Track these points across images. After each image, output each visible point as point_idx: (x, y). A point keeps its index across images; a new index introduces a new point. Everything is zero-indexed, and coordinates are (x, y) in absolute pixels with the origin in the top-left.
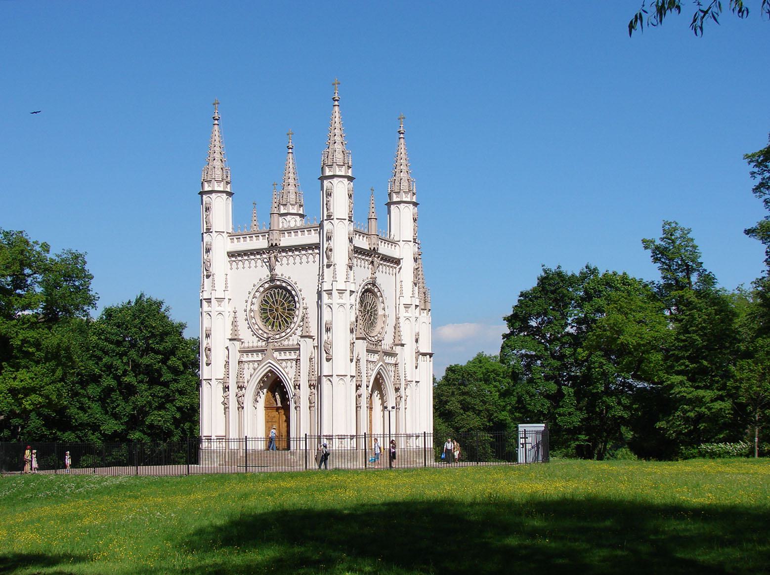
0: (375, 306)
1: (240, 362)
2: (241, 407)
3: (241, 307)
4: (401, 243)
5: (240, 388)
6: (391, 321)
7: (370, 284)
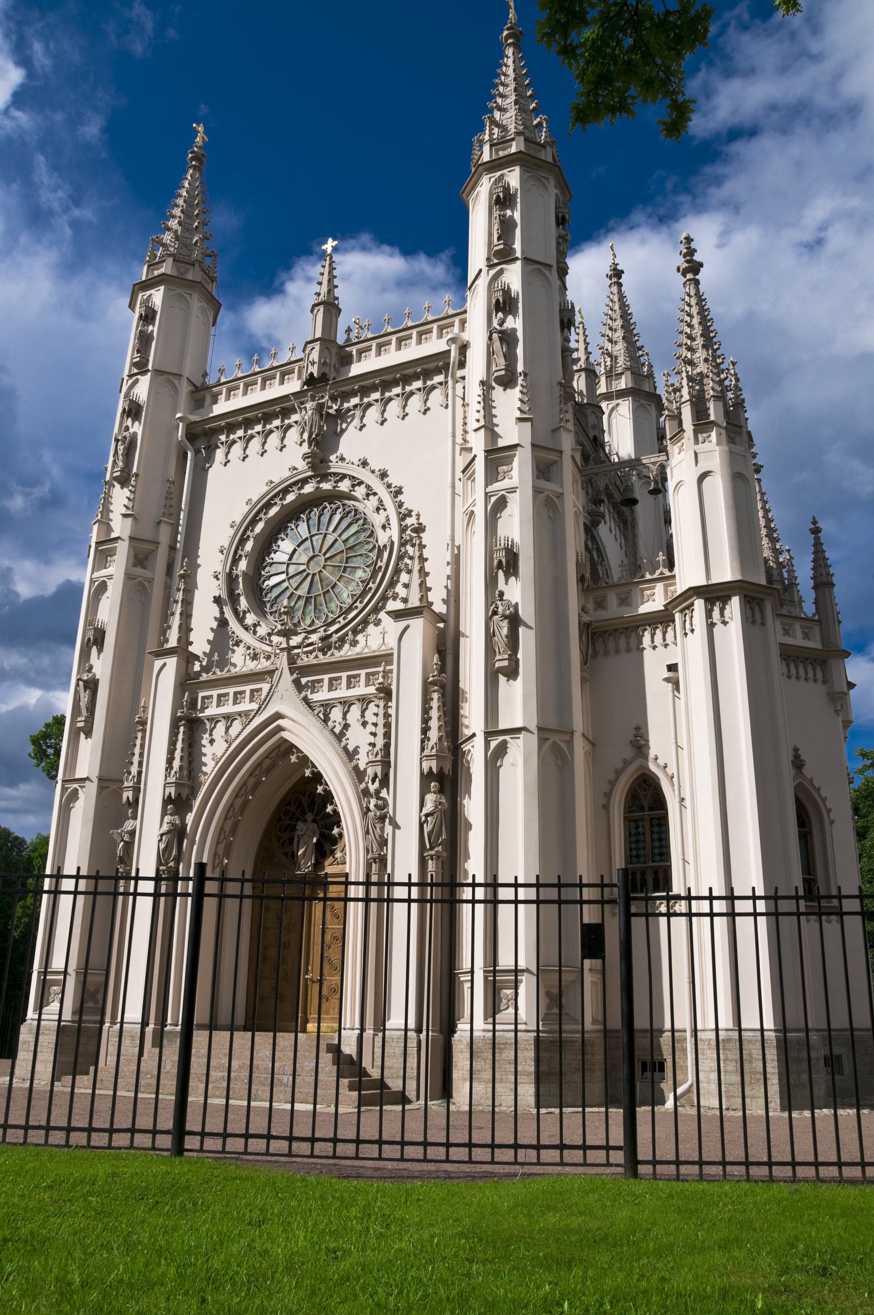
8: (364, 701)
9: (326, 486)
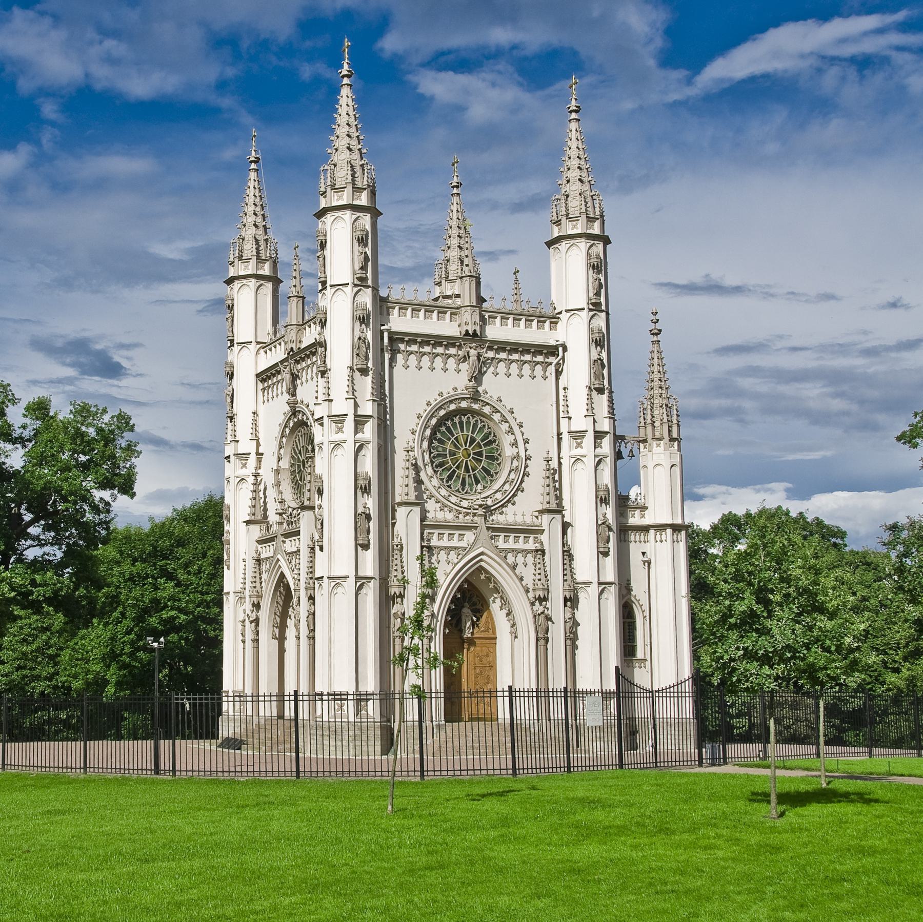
0: (491, 442)
1: (259, 561)
2: (256, 641)
3: (269, 462)
5: (257, 606)
6: (537, 469)
7: (463, 399)
8: (526, 552)
9: (476, 407)
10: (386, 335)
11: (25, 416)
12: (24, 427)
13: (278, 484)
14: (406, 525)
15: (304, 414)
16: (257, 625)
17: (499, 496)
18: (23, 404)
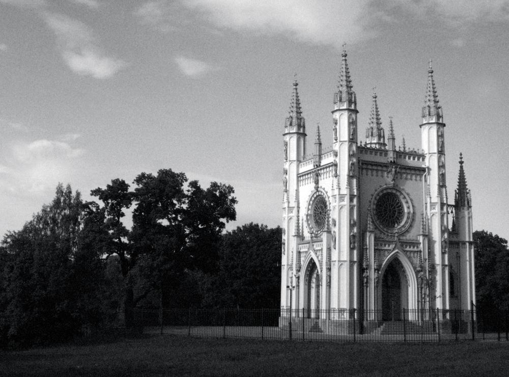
1: (299, 253)
3: (303, 212)
4: (427, 156)
5: (299, 271)
8: (415, 252)
9: (394, 192)
10: (361, 162)
11: (189, 186)
12: (188, 191)
13: (307, 220)
14: (370, 240)
15: (321, 192)
16: (299, 279)
17: (403, 229)
18: (189, 181)
